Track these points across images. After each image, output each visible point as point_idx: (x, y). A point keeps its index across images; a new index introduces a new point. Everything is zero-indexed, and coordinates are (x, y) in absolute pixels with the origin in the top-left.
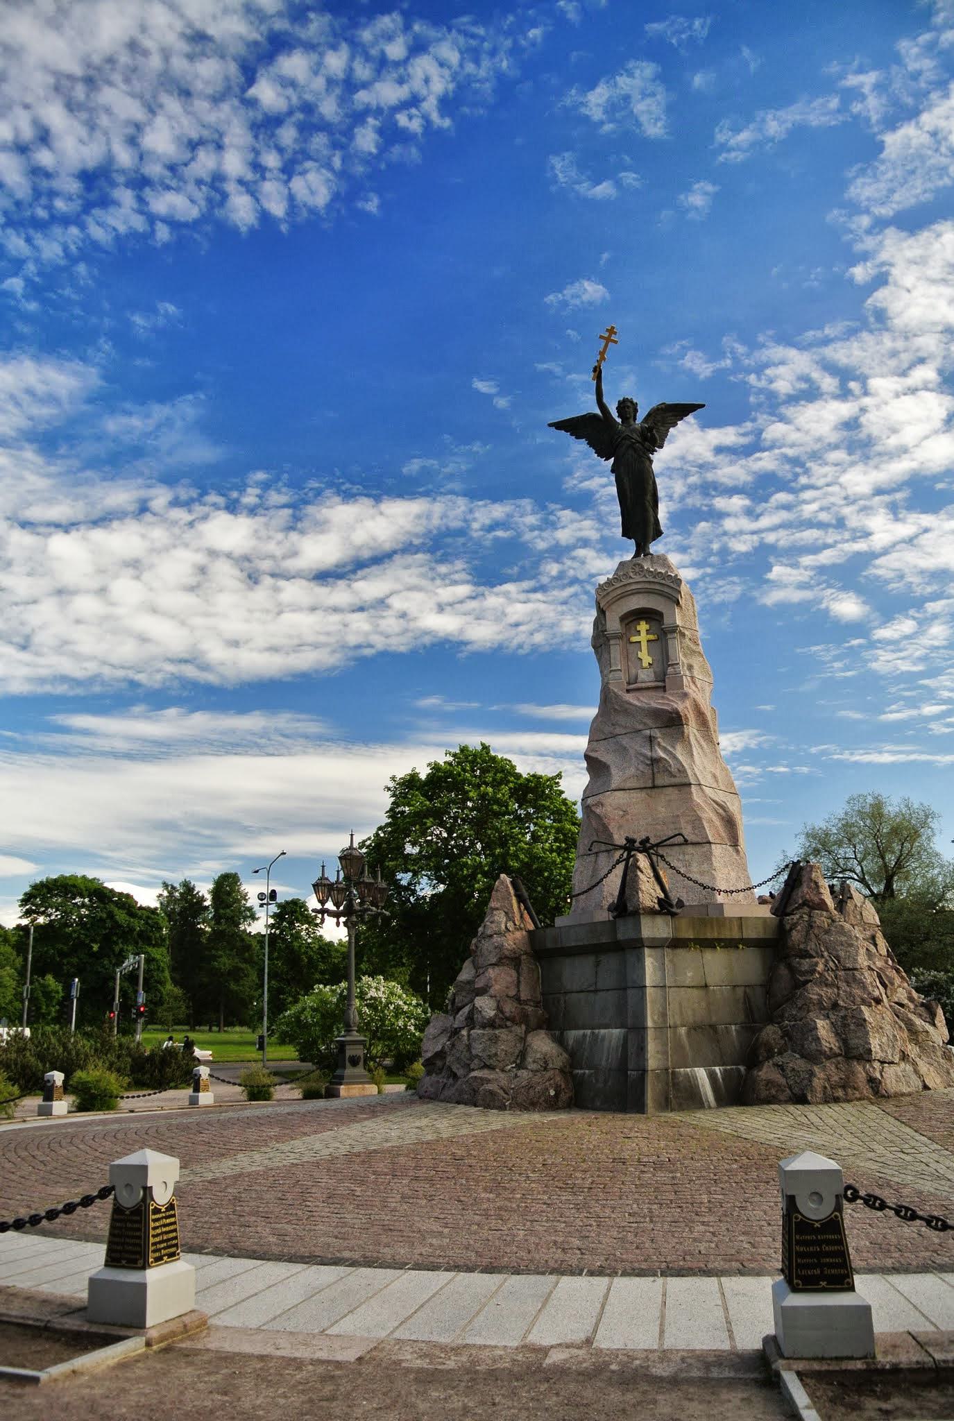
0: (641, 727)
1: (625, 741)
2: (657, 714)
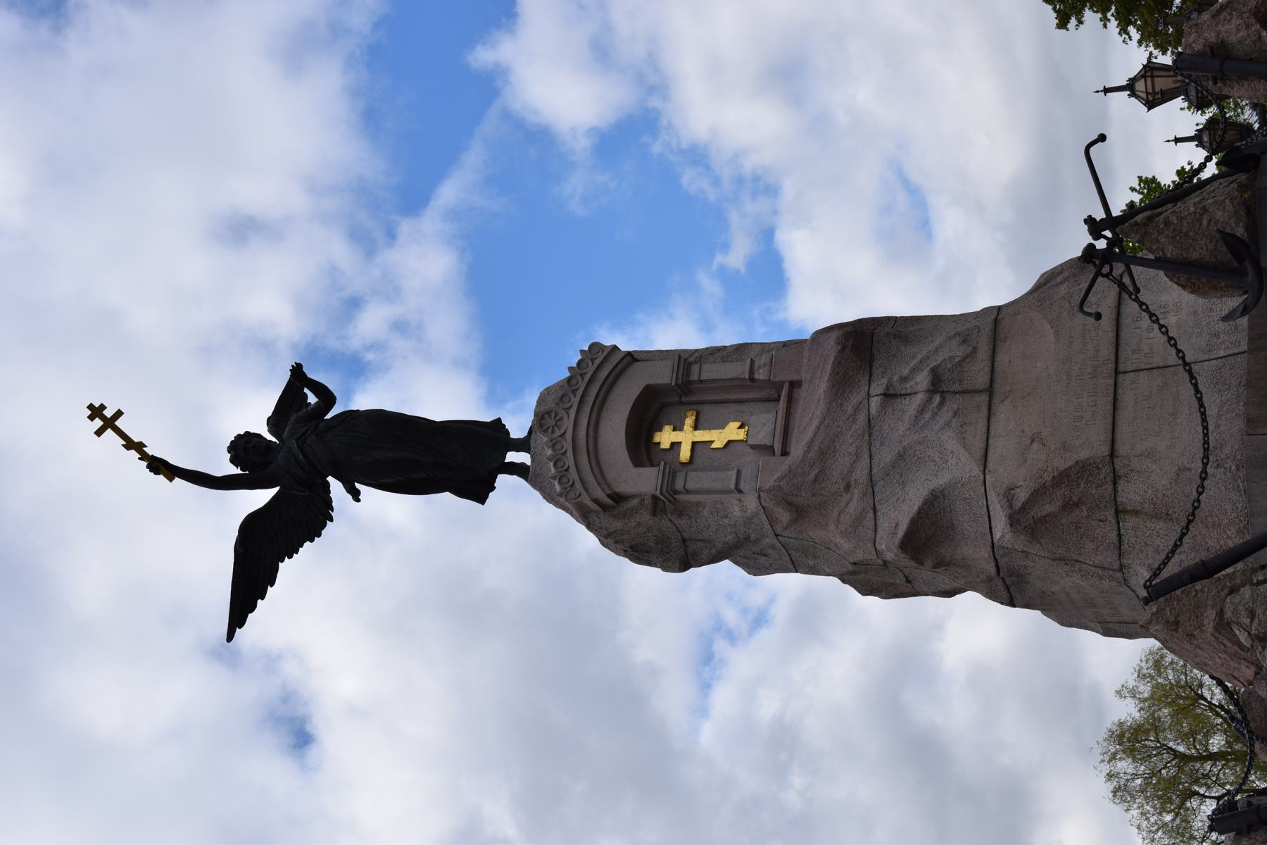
0: (862, 418)
1: (885, 456)
2: (841, 383)
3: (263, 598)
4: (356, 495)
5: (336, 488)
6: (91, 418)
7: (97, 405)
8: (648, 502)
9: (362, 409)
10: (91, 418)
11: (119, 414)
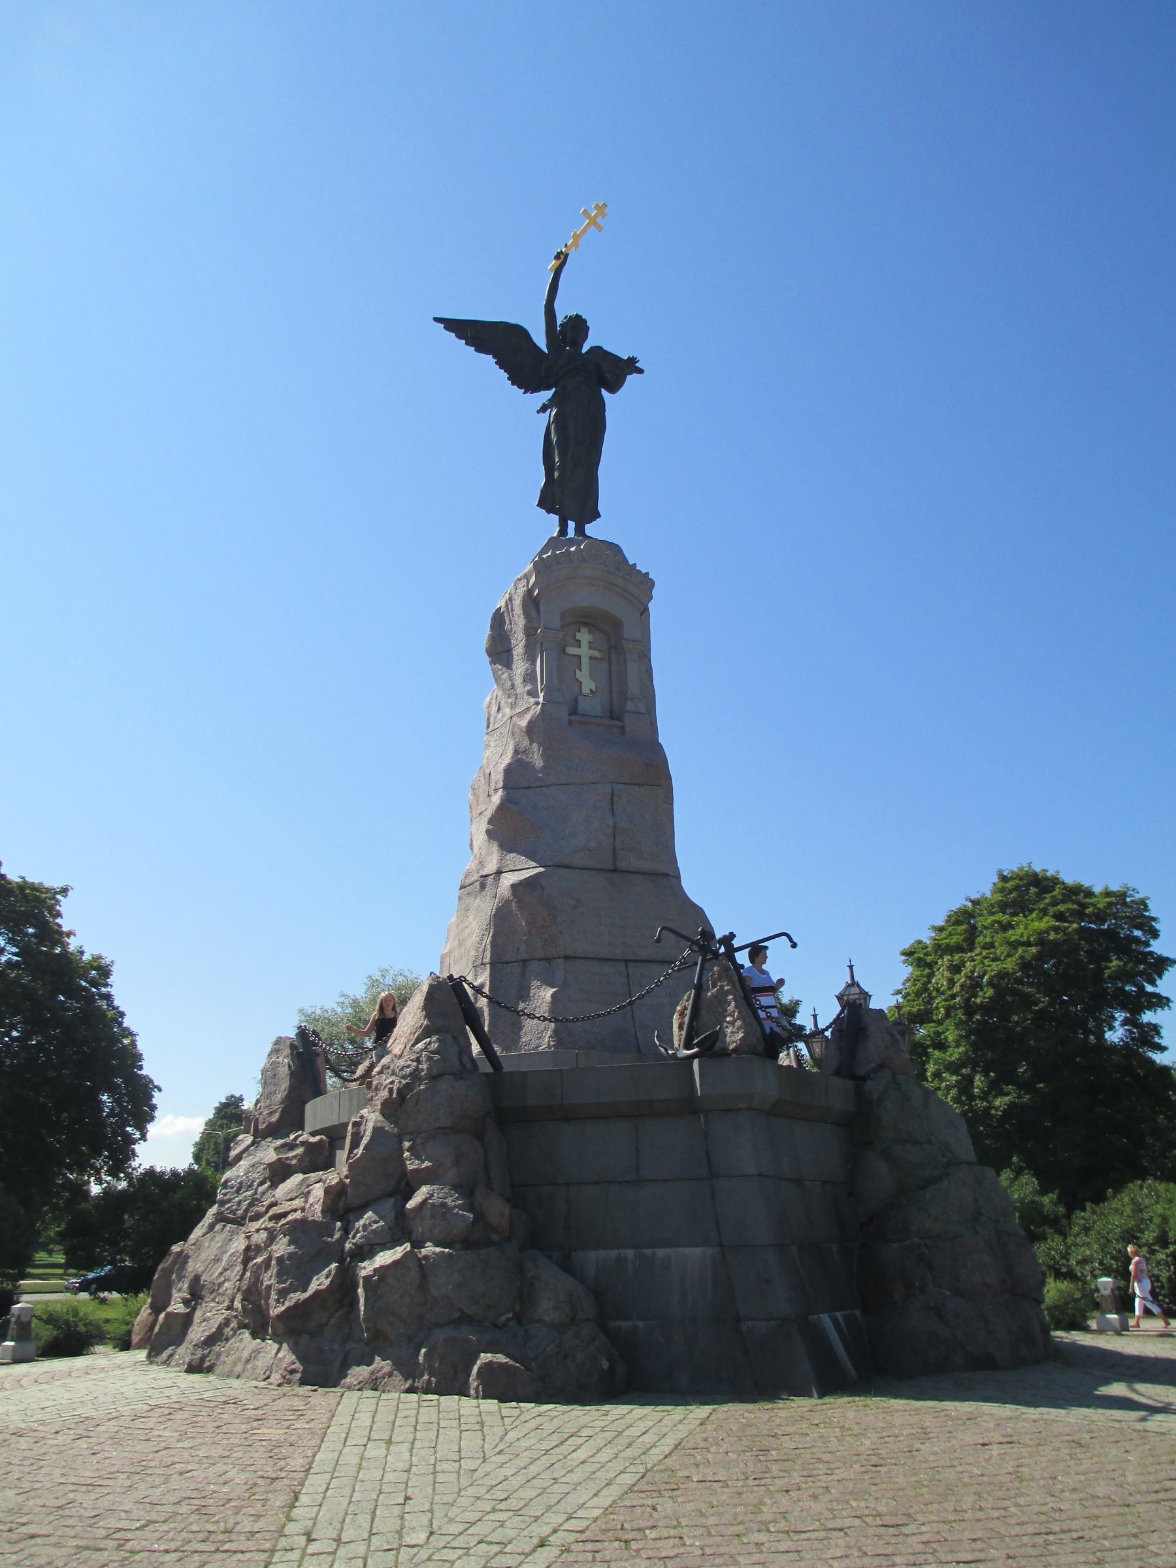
3: (467, 344)
4: (543, 409)
5: (548, 394)
7: (606, 211)
9: (606, 414)
11: (600, 229)
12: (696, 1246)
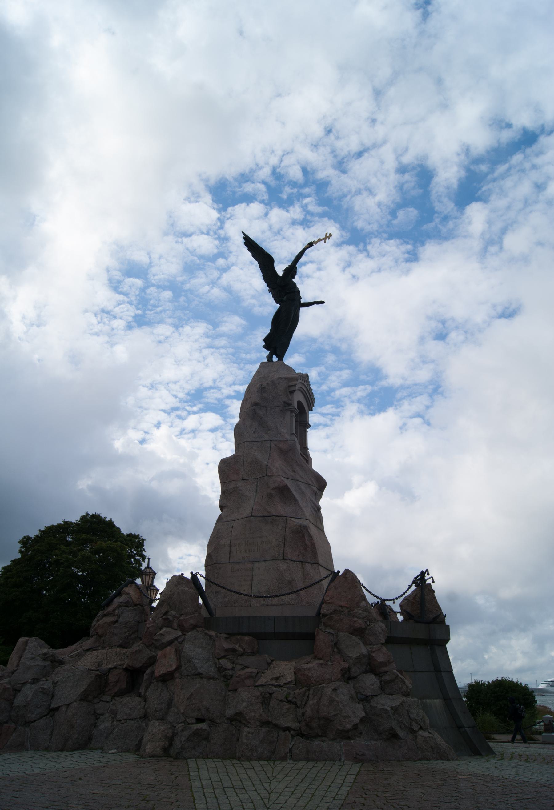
0: (310, 483)
1: (303, 487)
6: (330, 234)
8: (290, 402)
10: (330, 234)
12: (437, 699)
